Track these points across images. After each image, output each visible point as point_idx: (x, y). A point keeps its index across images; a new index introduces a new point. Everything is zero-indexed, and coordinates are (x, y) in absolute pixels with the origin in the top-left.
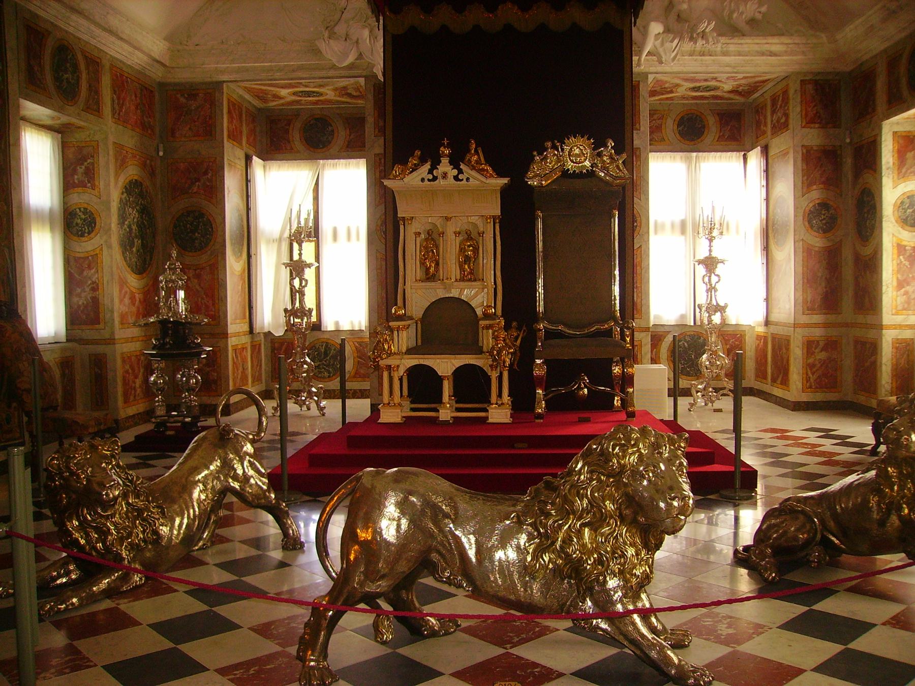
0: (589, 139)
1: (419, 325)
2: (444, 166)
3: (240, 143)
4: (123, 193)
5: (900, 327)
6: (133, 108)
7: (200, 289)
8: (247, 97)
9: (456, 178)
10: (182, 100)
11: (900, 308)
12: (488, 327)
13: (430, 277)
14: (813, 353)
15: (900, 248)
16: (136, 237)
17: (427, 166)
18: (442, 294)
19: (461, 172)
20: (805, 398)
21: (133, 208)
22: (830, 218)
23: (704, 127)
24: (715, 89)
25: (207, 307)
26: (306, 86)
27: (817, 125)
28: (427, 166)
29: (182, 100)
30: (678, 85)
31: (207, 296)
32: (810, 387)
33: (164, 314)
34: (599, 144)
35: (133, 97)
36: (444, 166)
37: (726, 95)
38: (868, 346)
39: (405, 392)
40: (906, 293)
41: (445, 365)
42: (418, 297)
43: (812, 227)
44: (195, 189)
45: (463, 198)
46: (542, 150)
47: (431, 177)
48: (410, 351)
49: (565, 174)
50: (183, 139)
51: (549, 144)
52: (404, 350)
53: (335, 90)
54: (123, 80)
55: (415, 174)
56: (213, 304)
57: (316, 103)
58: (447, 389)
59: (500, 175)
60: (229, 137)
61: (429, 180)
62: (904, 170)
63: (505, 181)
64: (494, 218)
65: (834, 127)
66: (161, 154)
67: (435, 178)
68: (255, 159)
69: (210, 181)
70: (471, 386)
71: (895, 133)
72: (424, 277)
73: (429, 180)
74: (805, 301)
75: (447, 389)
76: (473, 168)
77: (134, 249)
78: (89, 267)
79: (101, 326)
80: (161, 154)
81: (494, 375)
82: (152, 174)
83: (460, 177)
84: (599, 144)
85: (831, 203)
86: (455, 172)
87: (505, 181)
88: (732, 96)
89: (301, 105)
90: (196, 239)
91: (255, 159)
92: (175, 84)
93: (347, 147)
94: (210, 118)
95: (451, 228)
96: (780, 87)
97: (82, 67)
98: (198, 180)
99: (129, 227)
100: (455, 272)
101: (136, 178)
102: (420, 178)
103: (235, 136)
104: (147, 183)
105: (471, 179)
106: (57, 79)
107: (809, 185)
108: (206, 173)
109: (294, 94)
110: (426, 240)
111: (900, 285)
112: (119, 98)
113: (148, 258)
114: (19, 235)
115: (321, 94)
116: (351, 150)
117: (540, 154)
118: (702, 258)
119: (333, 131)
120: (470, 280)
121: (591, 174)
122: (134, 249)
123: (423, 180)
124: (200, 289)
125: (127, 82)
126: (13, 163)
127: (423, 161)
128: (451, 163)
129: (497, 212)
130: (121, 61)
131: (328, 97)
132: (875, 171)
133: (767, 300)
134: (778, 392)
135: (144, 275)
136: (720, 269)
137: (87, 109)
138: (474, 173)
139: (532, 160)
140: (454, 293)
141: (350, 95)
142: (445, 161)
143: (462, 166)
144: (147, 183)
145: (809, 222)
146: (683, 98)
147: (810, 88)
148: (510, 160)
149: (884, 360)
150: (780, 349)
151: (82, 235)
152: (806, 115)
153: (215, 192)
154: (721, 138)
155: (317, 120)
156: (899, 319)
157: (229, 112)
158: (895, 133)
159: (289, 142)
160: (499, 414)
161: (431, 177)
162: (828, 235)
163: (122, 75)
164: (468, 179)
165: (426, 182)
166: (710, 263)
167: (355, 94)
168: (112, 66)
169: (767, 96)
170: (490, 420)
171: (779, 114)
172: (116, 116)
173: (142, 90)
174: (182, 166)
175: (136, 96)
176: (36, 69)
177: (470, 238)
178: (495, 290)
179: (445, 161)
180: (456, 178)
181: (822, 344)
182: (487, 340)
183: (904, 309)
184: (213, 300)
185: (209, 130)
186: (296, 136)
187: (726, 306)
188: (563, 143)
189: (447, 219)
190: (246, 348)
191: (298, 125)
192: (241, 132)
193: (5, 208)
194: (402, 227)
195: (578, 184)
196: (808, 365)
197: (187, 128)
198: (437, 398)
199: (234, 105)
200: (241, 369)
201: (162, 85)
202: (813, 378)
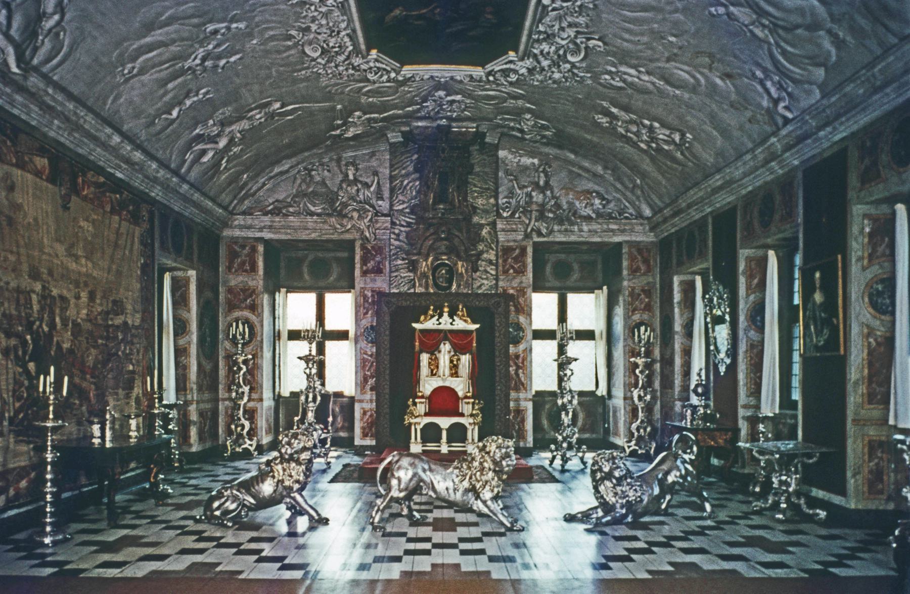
17: (437, 317)
18: (440, 383)
19: (454, 320)
48: (426, 415)
58: (444, 434)
59: (474, 322)
63: (477, 326)
67: (440, 324)
75: (444, 434)
87: (477, 326)
100: (447, 372)
140: (447, 384)
142: (446, 315)
143: (455, 318)
179: (446, 315)
180: (451, 324)
182: (466, 408)
191: (306, 264)
198: (438, 440)
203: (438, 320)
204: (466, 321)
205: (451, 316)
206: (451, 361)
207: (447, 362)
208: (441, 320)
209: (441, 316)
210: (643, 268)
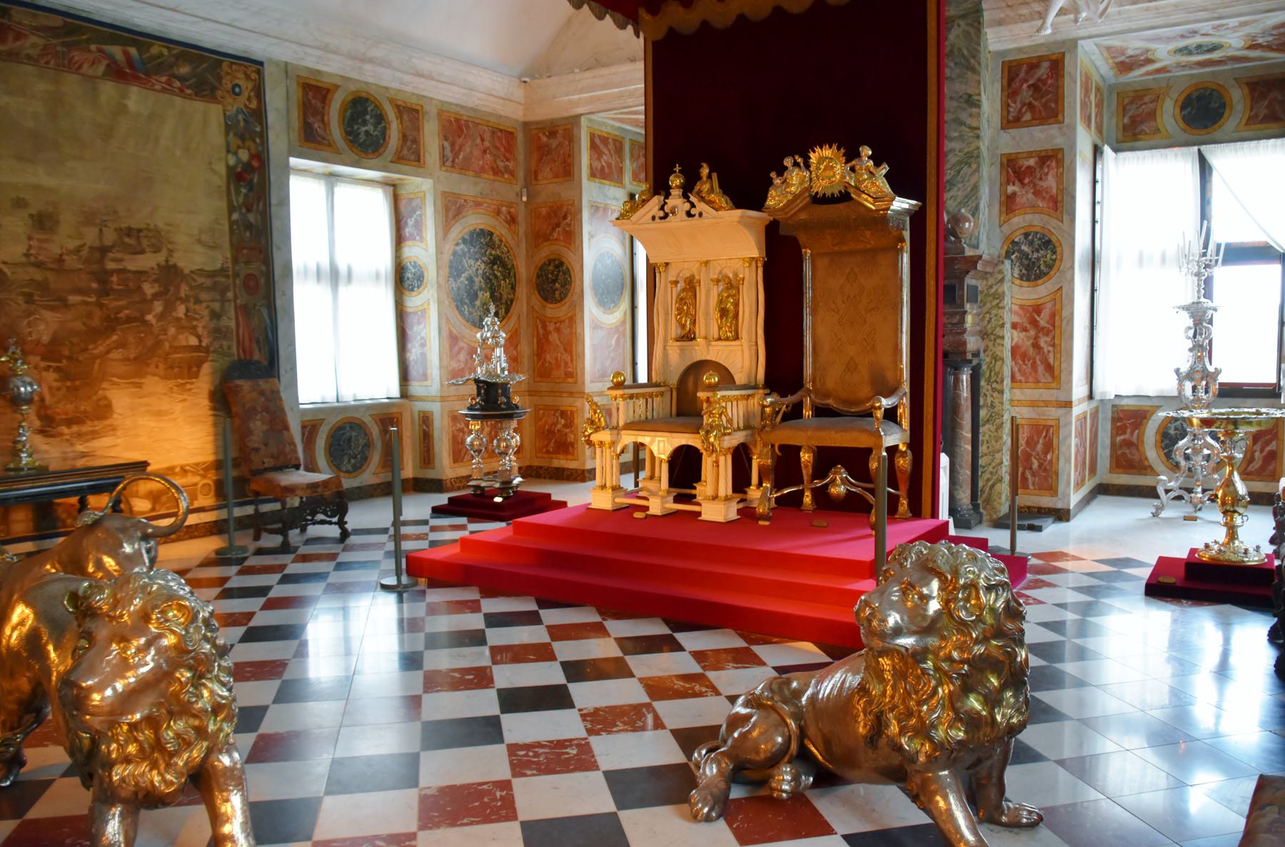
2: (676, 200)
3: (619, 182)
4: (457, 244)
6: (477, 153)
16: (481, 289)
19: (693, 206)
23: (1223, 106)
25: (566, 363)
29: (544, 139)
31: (566, 350)
34: (852, 155)
35: (478, 141)
36: (676, 200)
44: (555, 235)
46: (781, 170)
47: (661, 214)
52: (621, 424)
54: (458, 127)
60: (593, 175)
64: (756, 260)
66: (524, 199)
67: (666, 216)
69: (569, 225)
73: (661, 218)
76: (702, 199)
77: (478, 303)
78: (419, 323)
79: (428, 383)
82: (512, 220)
84: (852, 155)
86: (687, 206)
92: (537, 123)
97: (391, 114)
98: (558, 225)
99: (470, 280)
101: (482, 227)
102: (650, 215)
103: (598, 174)
104: (500, 230)
106: (351, 135)
108: (565, 217)
110: (684, 290)
112: (452, 145)
114: (284, 293)
117: (780, 174)
121: (845, 197)
122: (478, 303)
123: (654, 218)
125: (467, 127)
126: (276, 224)
130: (457, 105)
137: (399, 159)
139: (770, 183)
142: (676, 192)
143: (692, 199)
144: (500, 230)
151: (412, 290)
154: (1251, 120)
157: (593, 146)
163: (457, 120)
164: (700, 215)
168: (440, 114)
170: (704, 517)
172: (449, 163)
173: (493, 133)
174: (544, 211)
175: (483, 140)
176: (316, 126)
179: (676, 192)
180: (689, 214)
185: (567, 170)
193: (264, 268)
199: (605, 140)
201: (526, 125)
203: (662, 208)
205: (687, 190)
209: (667, 195)
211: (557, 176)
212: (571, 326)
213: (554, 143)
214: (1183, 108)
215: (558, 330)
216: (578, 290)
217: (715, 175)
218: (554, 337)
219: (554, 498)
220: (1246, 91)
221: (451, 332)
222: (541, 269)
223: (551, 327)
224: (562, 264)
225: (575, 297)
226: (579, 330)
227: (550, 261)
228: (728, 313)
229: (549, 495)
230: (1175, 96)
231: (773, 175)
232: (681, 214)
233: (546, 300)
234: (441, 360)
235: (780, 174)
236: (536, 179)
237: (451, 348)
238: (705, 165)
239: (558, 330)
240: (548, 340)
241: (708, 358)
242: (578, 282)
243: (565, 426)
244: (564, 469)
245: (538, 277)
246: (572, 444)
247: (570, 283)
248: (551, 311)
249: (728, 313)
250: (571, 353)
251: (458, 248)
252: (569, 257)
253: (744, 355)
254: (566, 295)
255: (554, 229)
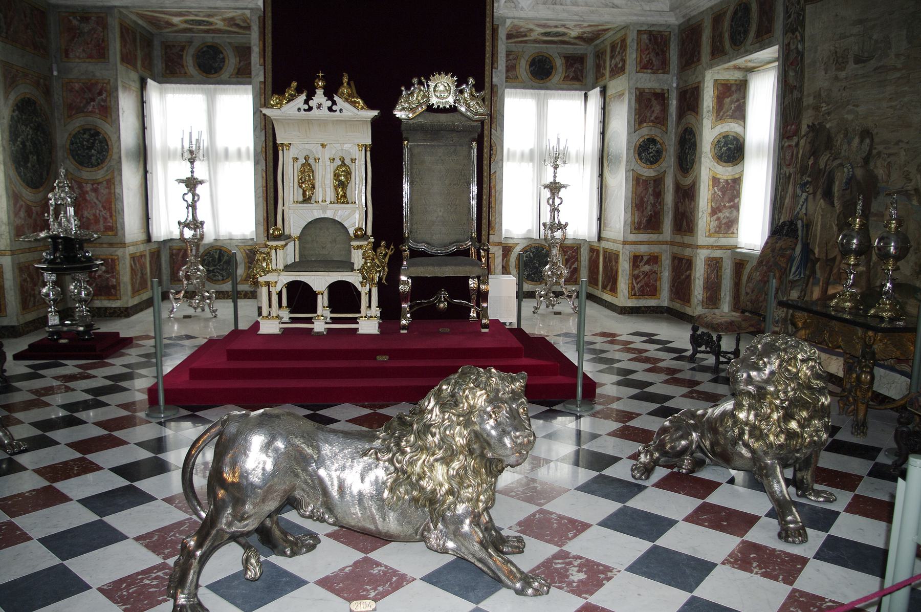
0: (452, 76)
1: (297, 242)
2: (320, 97)
3: (135, 67)
4: (14, 111)
5: (712, 247)
7: (97, 202)
8: (140, 22)
9: (330, 109)
10: (75, 22)
11: (712, 231)
12: (359, 247)
13: (307, 200)
14: (638, 266)
15: (715, 181)
17: (303, 97)
18: (318, 214)
19: (334, 103)
20: (631, 303)
21: (26, 126)
22: (657, 152)
23: (552, 68)
24: (564, 34)
26: (196, 15)
27: (649, 71)
28: (303, 97)
29: (75, 22)
30: (531, 30)
31: (104, 208)
32: (635, 295)
33: (55, 229)
36: (320, 97)
37: (573, 41)
38: (684, 262)
39: (284, 302)
40: (718, 219)
41: (320, 281)
42: (296, 218)
43: (641, 159)
44: (90, 108)
45: (334, 131)
47: (306, 107)
48: (288, 268)
49: (430, 109)
50: (77, 60)
51: (415, 80)
52: (282, 268)
53: (224, 20)
55: (292, 104)
56: (111, 216)
57: (207, 31)
58: (322, 301)
59: (371, 106)
61: (305, 110)
62: (721, 114)
63: (375, 113)
65: (664, 73)
67: (310, 109)
68: (149, 81)
69: (105, 101)
70: (344, 298)
71: (715, 81)
72: (301, 199)
73: (305, 110)
74: (633, 223)
75: (322, 301)
77: (29, 165)
80: (55, 73)
81: (364, 291)
83: (334, 108)
85: (658, 139)
86: (329, 103)
87: (375, 113)
88: (577, 41)
89: (193, 32)
90: (93, 155)
91: (149, 81)
92: (67, 7)
93: (237, 74)
94: (103, 41)
95: (326, 154)
96: (619, 35)
98: (93, 100)
99: (23, 143)
100: (330, 195)
101: (28, 96)
105: (344, 111)
107: (641, 123)
108: (100, 94)
109: (186, 22)
111: (714, 212)
113: (45, 173)
115: (211, 24)
116: (241, 76)
117: (408, 89)
118: (548, 182)
119: (224, 58)
120: (343, 203)
121: (453, 109)
123: (299, 109)
124: (97, 202)
127: (299, 91)
128: (325, 94)
129: (369, 141)
131: (217, 26)
132: (697, 113)
133: (600, 219)
134: (607, 297)
135: (41, 189)
136: (563, 193)
138: (346, 106)
140: (329, 214)
141: (238, 25)
142: (320, 92)
143: (336, 98)
145: (639, 154)
146: (535, 41)
147: (645, 37)
148: (380, 94)
149: (698, 275)
150: (610, 261)
152: (641, 62)
153: (109, 111)
154: (566, 78)
155: (208, 47)
156: (711, 241)
158: (715, 81)
159: (183, 67)
160: (368, 324)
161: (306, 107)
162: (655, 166)
164: (341, 110)
165: (303, 112)
166: (555, 188)
167: (242, 24)
169: (608, 43)
170: (361, 332)
171: (617, 60)
174: (77, 86)
175: (25, 17)
177: (343, 164)
178: (366, 212)
179: (320, 92)
180: (330, 109)
181: (645, 259)
183: (716, 232)
184: (111, 213)
186: (189, 62)
187: (566, 224)
188: (428, 79)
189: (323, 146)
190: (145, 256)
192: (136, 56)
194: (280, 152)
195: (443, 118)
196: (633, 276)
197: (80, 50)
200: (139, 275)
202: (637, 287)
203: (306, 102)
204: (354, 104)
206: (337, 176)
207: (330, 177)
208: (311, 103)
210: (656, 62)
211: (90, 57)
212: (109, 187)
213: (86, 28)
214: (531, 66)
215: (95, 190)
216: (115, 157)
217: (352, 83)
218: (91, 196)
219: (122, 335)
220: (564, 61)
221: (14, 191)
222: (74, 136)
223: (88, 188)
224: (97, 133)
225: (113, 163)
226: (117, 191)
227: (85, 131)
228: (342, 183)
229: (118, 334)
230: (527, 58)
231: (403, 88)
232: (325, 110)
233: (81, 163)
234: (9, 217)
235: (408, 89)
236: (67, 56)
237: (15, 205)
238: (346, 75)
239: (95, 190)
240: (85, 199)
241: (326, 216)
242: (115, 150)
243: (106, 272)
244: (106, 308)
245: (72, 143)
246: (114, 287)
247: (107, 151)
248: (86, 174)
249: (342, 183)
250: (110, 209)
251: (15, 114)
252: (105, 127)
253: (355, 215)
254: (103, 161)
255: (88, 103)
